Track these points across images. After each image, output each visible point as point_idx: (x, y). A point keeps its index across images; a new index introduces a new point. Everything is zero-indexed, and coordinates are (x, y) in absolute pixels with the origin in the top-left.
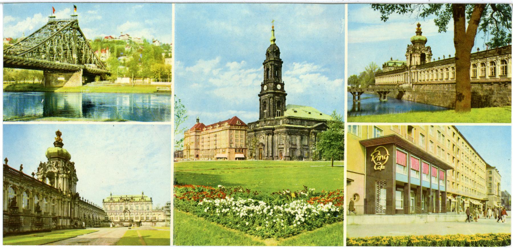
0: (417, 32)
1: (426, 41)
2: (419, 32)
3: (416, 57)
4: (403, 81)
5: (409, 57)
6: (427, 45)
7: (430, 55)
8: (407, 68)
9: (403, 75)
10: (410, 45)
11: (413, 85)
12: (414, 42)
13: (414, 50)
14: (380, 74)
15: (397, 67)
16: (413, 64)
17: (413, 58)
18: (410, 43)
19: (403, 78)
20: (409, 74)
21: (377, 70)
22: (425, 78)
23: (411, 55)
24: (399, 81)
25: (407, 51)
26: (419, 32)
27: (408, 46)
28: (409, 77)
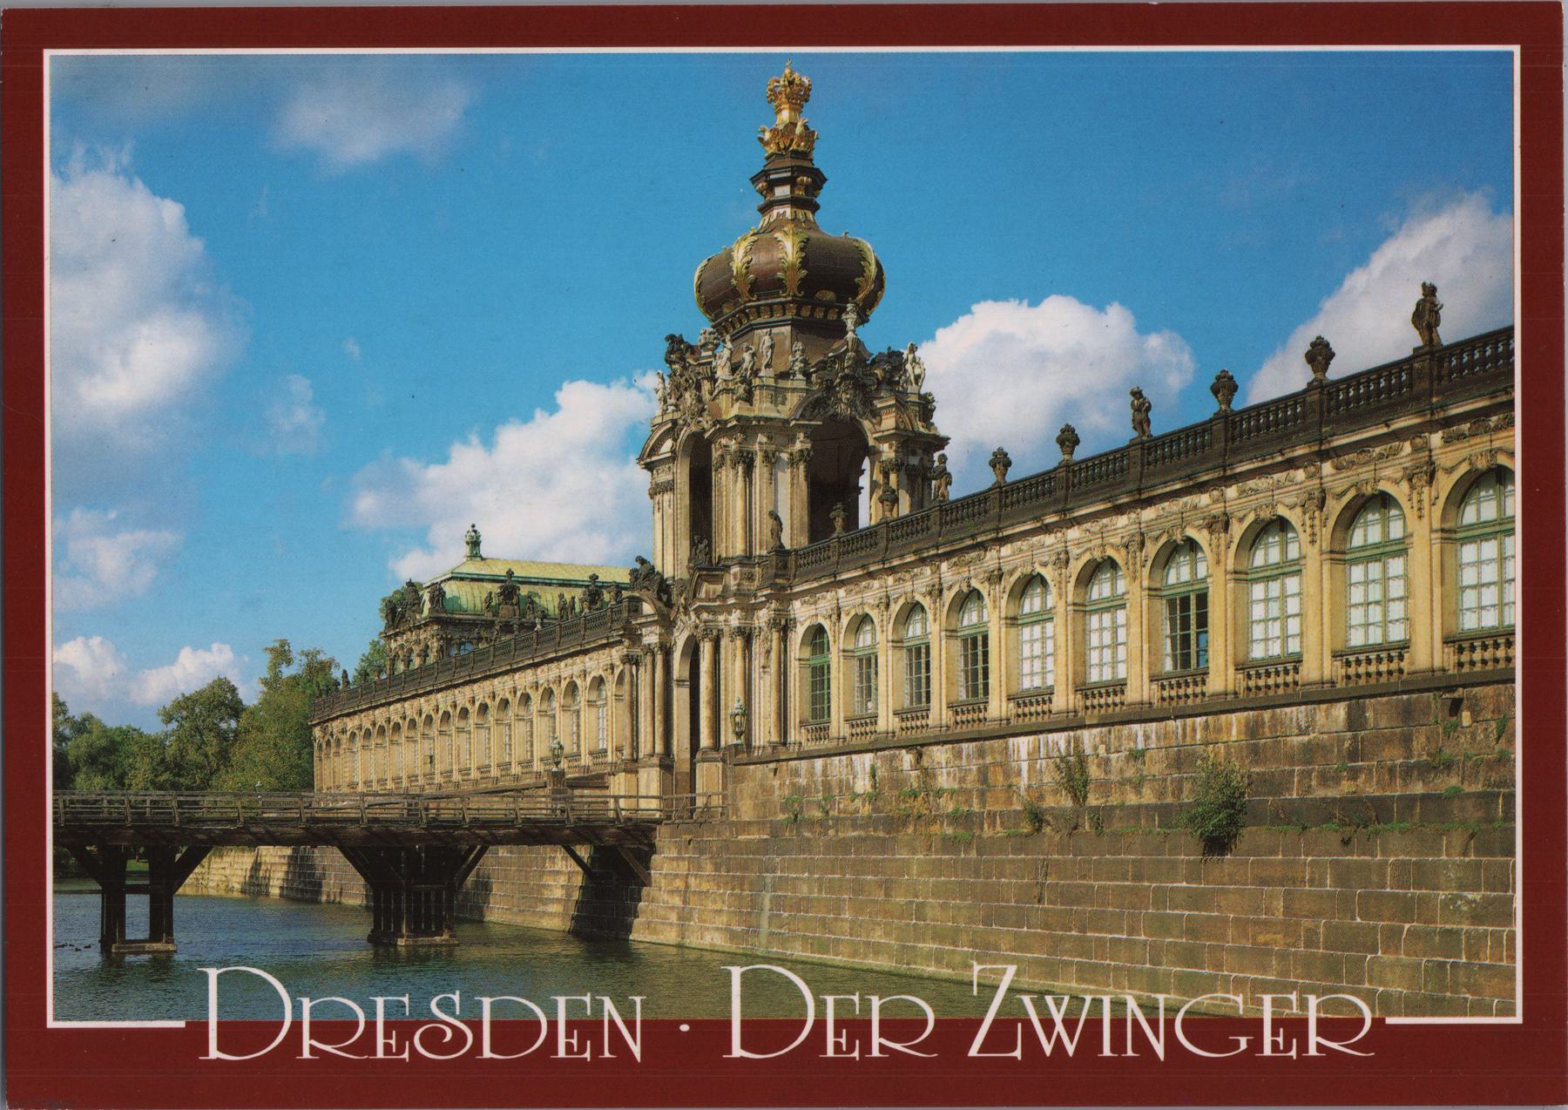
3: (760, 469)
5: (681, 474)
24: (569, 749)
27: (675, 342)
28: (681, 696)
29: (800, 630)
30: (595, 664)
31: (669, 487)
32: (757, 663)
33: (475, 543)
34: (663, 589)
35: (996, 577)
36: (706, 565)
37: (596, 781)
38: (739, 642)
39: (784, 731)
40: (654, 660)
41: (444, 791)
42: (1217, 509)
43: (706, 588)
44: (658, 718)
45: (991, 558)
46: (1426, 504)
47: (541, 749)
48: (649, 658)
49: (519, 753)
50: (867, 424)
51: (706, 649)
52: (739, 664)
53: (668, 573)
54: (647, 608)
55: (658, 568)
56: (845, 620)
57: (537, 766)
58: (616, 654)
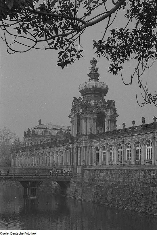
0: (90, 75)
1: (105, 91)
2: (94, 75)
4: (64, 161)
5: (75, 119)
6: (107, 98)
10: (78, 98)
13: (86, 107)
15: (50, 136)
16: (83, 131)
17: (83, 122)
18: (78, 95)
19: (64, 157)
21: (12, 141)
23: (79, 116)
28: (75, 156)
29: (94, 147)
30: (61, 148)
31: (73, 121)
32: (87, 152)
33: (40, 122)
34: (72, 138)
35: (123, 142)
36: (79, 135)
37: (61, 168)
39: (91, 163)
40: (71, 150)
41: (38, 168)
42: (153, 137)
43: (80, 139)
44: (71, 159)
45: (122, 140)
48: (70, 149)
50: (106, 113)
52: (84, 152)
53: (73, 135)
54: (70, 141)
55: (71, 134)
58: (65, 147)
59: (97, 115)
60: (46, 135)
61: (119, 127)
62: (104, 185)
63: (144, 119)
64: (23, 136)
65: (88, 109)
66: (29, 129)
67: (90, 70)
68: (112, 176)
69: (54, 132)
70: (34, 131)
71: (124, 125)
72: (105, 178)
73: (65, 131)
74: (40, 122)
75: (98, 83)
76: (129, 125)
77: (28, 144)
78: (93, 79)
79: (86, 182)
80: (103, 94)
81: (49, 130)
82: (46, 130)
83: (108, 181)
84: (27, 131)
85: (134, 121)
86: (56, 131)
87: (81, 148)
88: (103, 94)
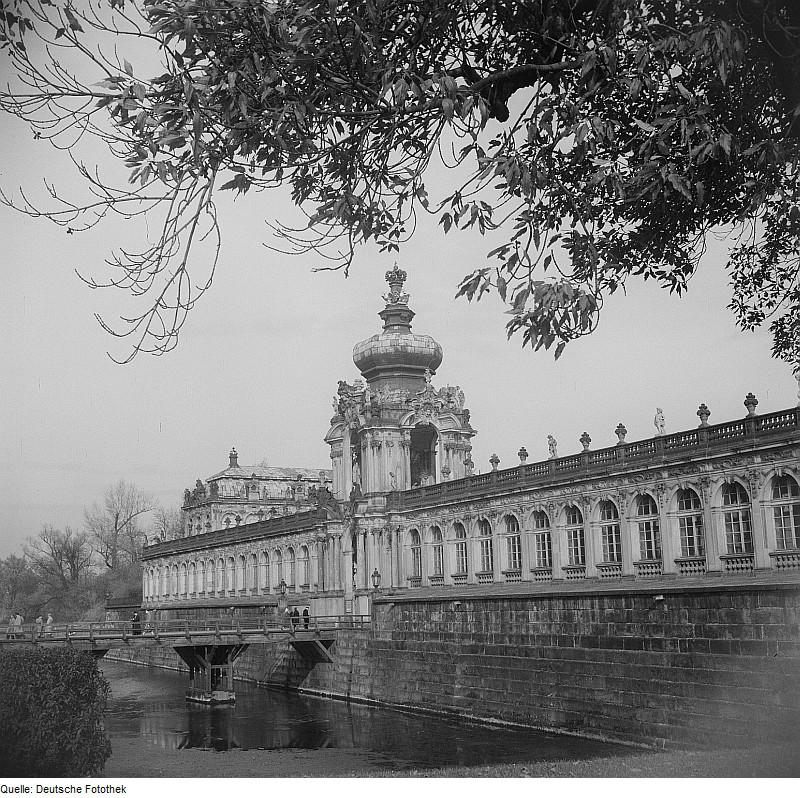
1: (433, 361)
2: (397, 316)
4: (315, 580)
5: (347, 446)
6: (438, 381)
7: (465, 432)
8: (336, 508)
9: (313, 552)
11: (376, 603)
12: (371, 366)
14: (161, 551)
18: (354, 376)
19: (315, 563)
20: (347, 543)
22: (440, 564)
23: (357, 437)
24: (288, 583)
25: (333, 413)
26: (397, 316)
31: (340, 455)
33: (233, 457)
38: (377, 535)
46: (664, 502)
47: (275, 582)
49: (263, 584)
51: (361, 538)
56: (427, 528)
57: (272, 592)
59: (413, 433)
60: (252, 497)
61: (482, 467)
62: (443, 648)
63: (552, 444)
64: (181, 502)
65: (385, 415)
66: (199, 481)
67: (386, 300)
68: (465, 620)
69: (277, 490)
70: (214, 488)
71: (495, 461)
72: (442, 627)
73: (311, 485)
74: (233, 457)
75: (410, 337)
76: (511, 461)
77: (199, 528)
78: (396, 328)
79: (385, 643)
80: (428, 371)
81: (262, 484)
82: (252, 482)
83: (452, 636)
84: (192, 487)
85: (523, 450)
86: (284, 486)
87: (365, 537)
88: (428, 371)
